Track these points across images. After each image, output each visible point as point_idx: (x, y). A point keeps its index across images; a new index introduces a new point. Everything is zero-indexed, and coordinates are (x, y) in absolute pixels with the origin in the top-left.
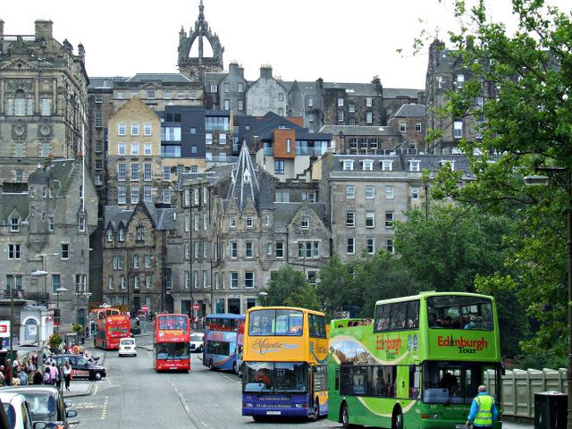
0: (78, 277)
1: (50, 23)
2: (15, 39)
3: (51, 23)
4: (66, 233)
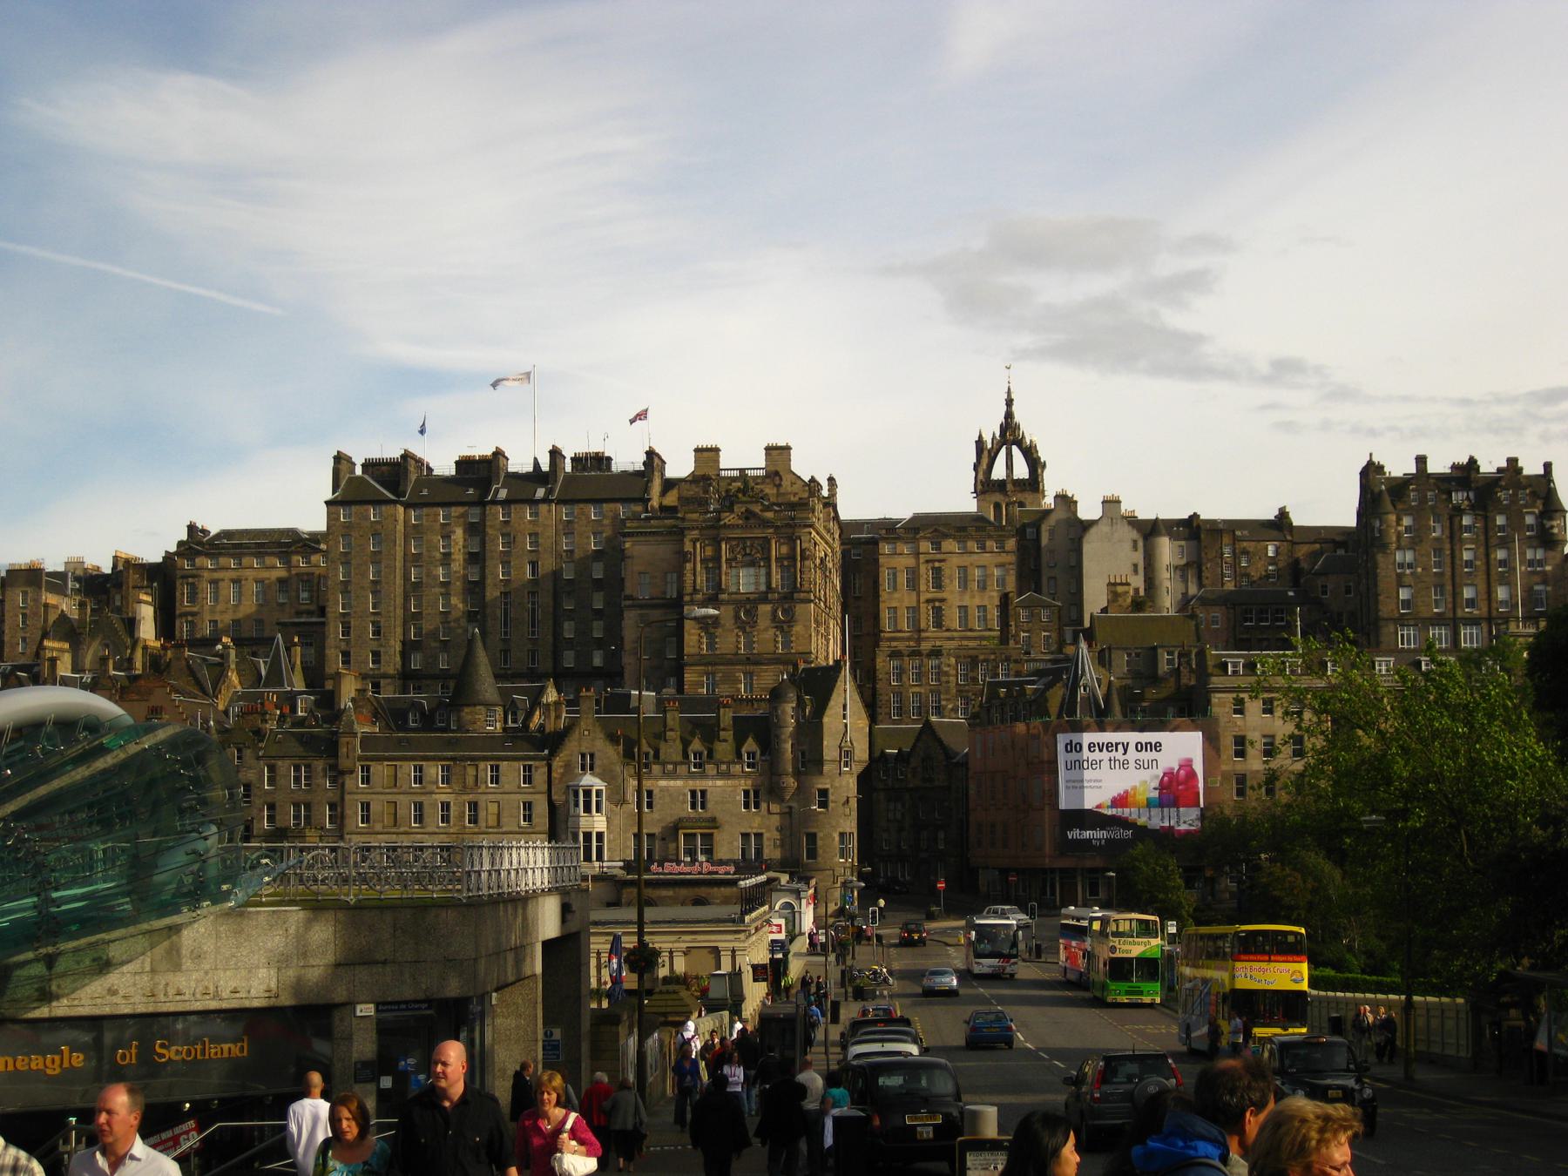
1: (788, 448)
2: (736, 473)
3: (788, 448)
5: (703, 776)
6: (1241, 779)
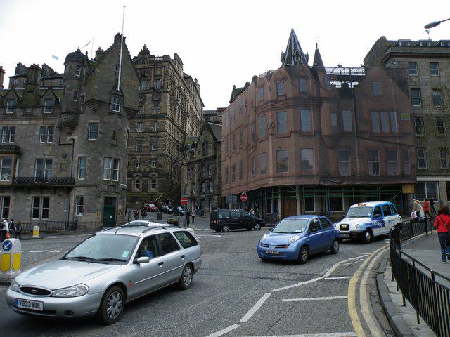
4: (95, 111)
5: (13, 117)
6: (418, 119)
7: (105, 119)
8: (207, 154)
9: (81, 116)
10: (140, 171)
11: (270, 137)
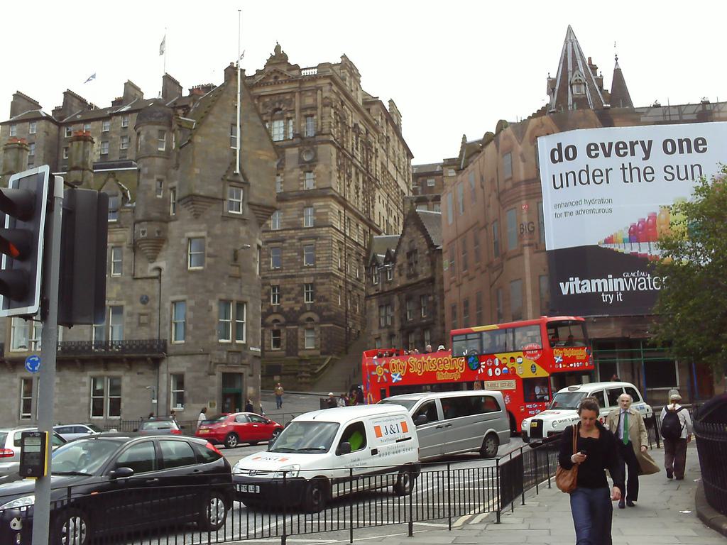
0: (226, 303)
4: (197, 216)
7: (217, 230)
8: (416, 275)
9: (172, 225)
10: (280, 311)
11: (527, 250)
